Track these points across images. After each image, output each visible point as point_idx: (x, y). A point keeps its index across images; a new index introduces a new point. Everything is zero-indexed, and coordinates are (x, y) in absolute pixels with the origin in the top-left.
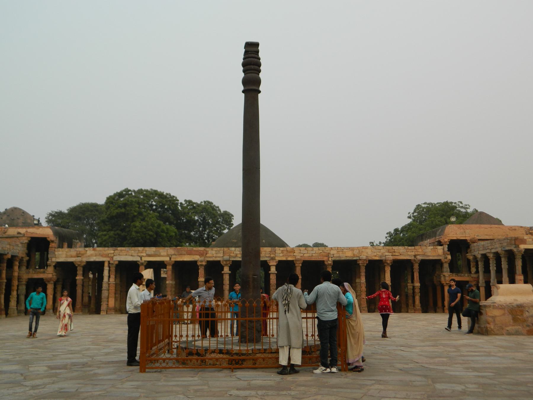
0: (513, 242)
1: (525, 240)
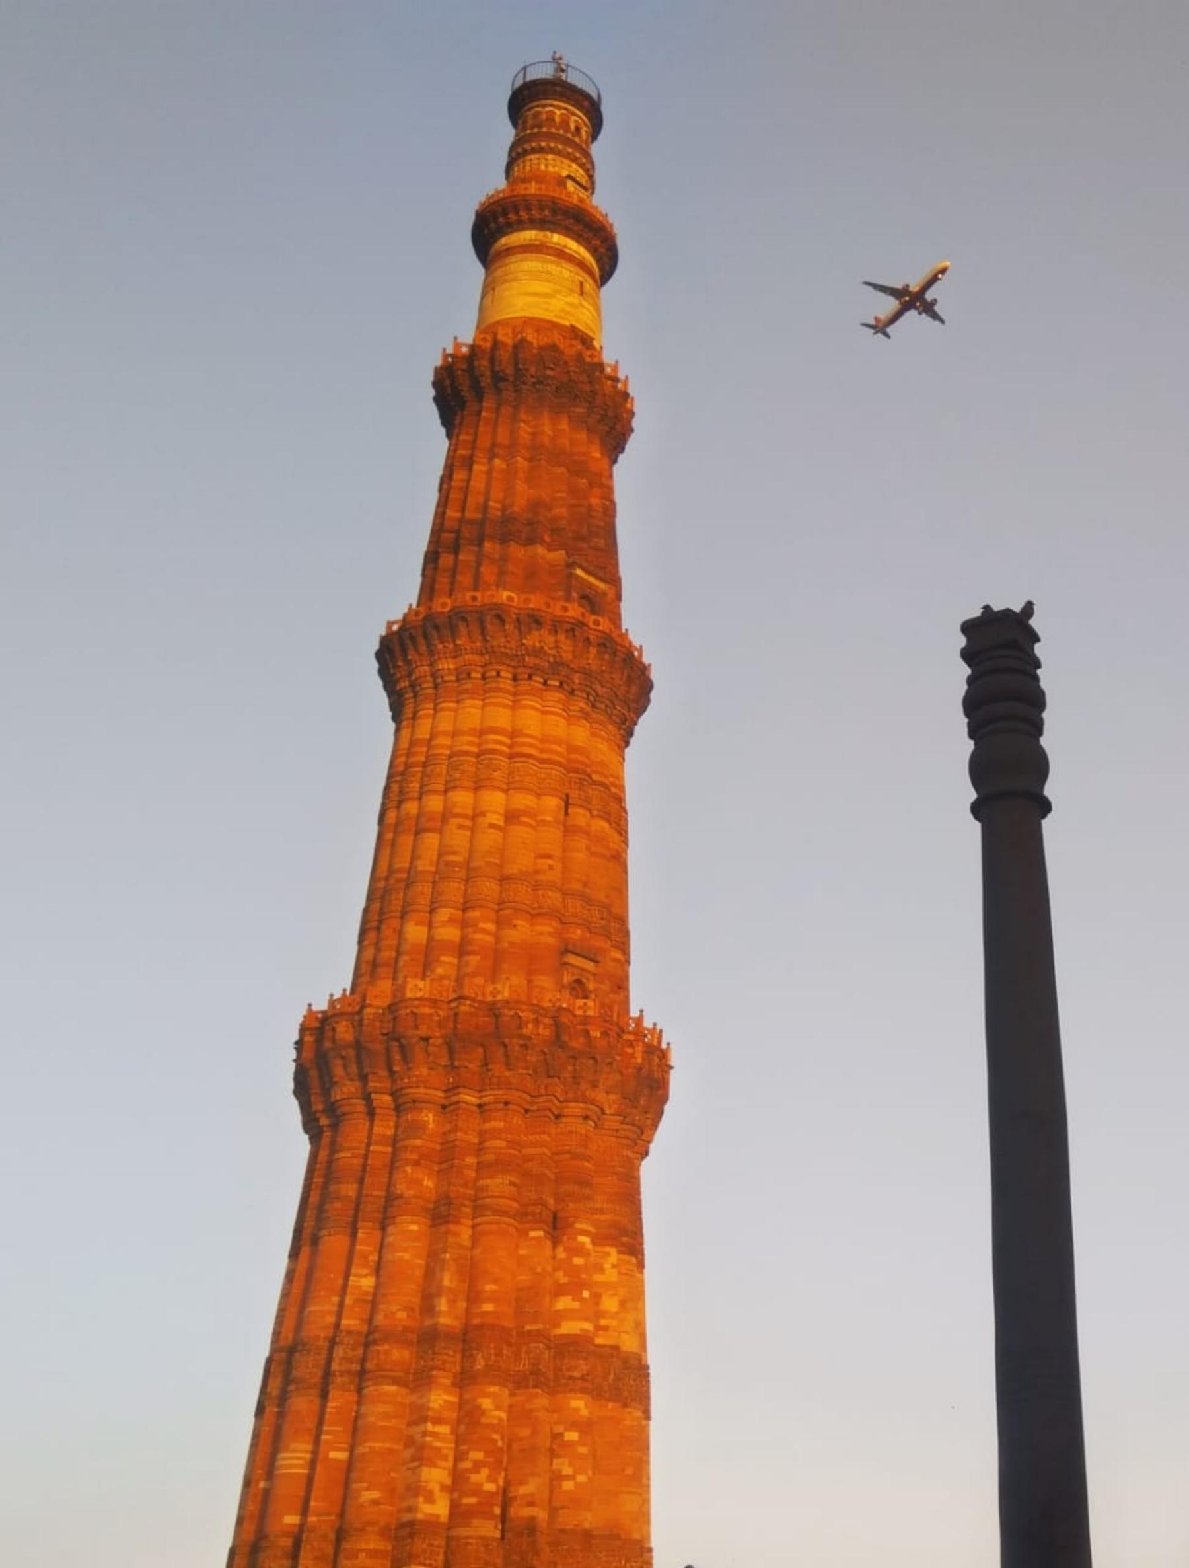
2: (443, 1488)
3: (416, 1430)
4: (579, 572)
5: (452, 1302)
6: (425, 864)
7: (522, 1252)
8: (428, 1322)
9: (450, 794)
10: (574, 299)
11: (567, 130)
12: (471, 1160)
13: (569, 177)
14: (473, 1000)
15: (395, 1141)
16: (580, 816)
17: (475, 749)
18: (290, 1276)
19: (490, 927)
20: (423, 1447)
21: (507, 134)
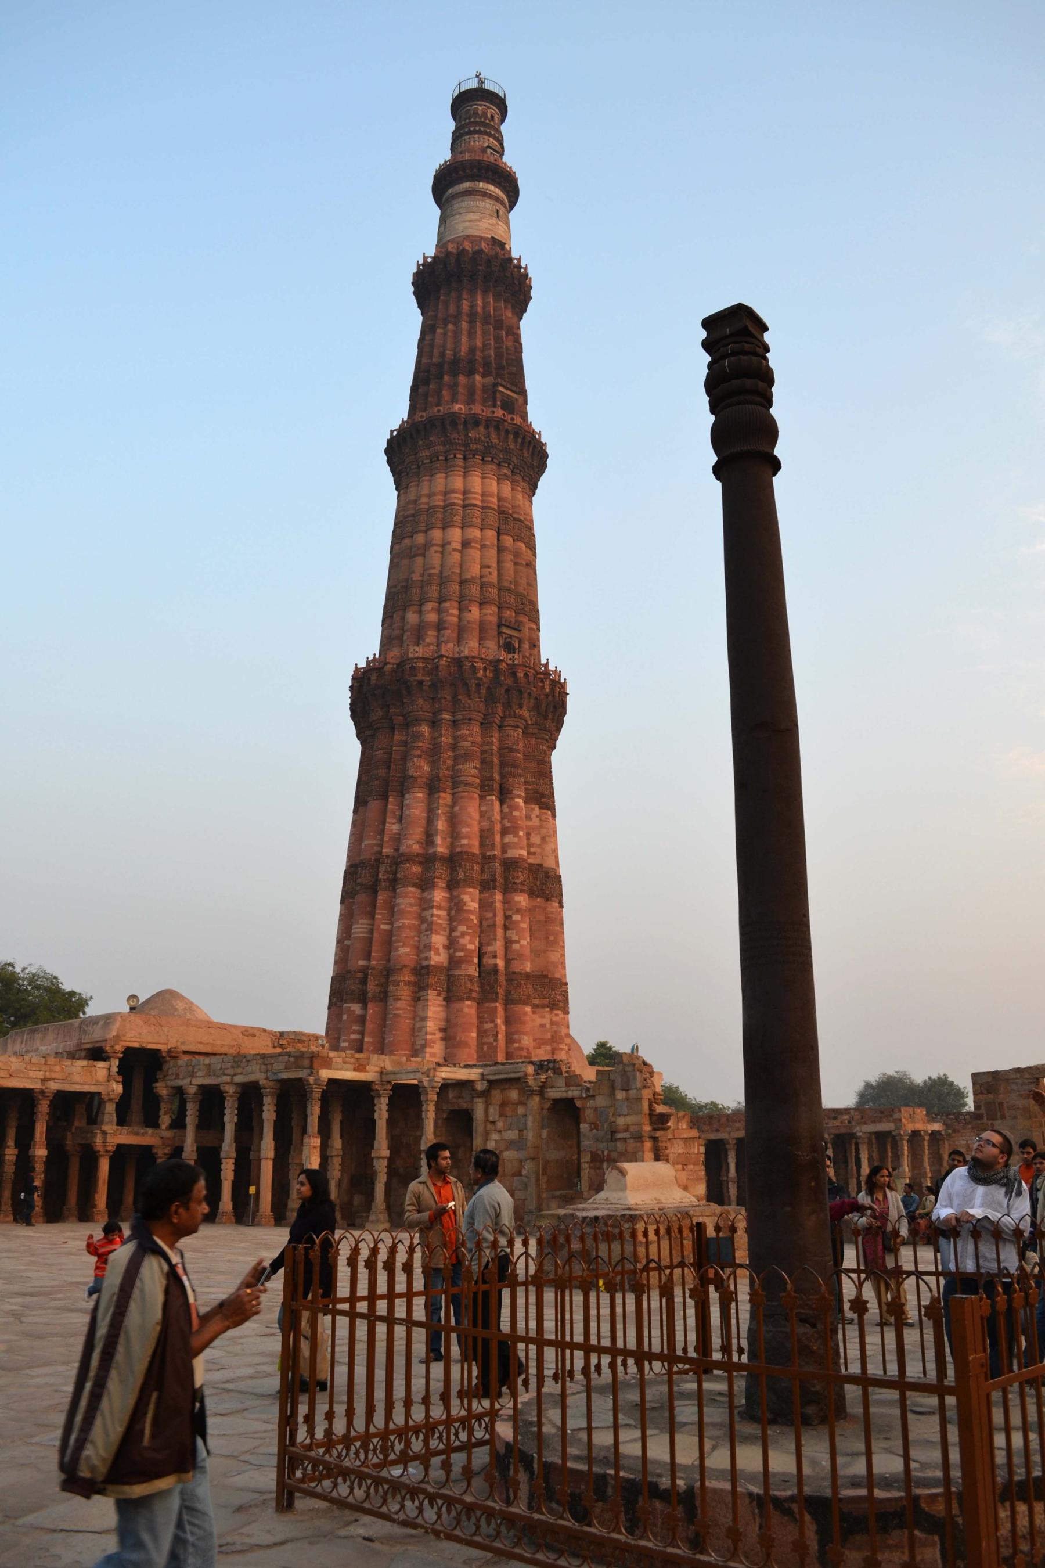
0: (306, 1062)
1: (331, 1059)
2: (445, 947)
3: (427, 913)
4: (501, 389)
5: (444, 839)
6: (416, 577)
7: (483, 809)
8: (431, 851)
9: (429, 532)
10: (494, 221)
11: (486, 118)
12: (450, 754)
13: (488, 147)
14: (447, 657)
15: (405, 744)
16: (508, 541)
17: (442, 504)
18: (354, 823)
19: (455, 612)
20: (432, 923)
21: (452, 125)
